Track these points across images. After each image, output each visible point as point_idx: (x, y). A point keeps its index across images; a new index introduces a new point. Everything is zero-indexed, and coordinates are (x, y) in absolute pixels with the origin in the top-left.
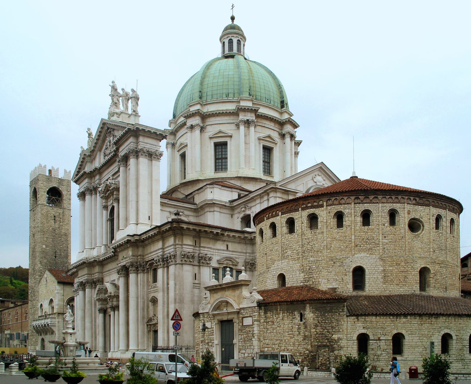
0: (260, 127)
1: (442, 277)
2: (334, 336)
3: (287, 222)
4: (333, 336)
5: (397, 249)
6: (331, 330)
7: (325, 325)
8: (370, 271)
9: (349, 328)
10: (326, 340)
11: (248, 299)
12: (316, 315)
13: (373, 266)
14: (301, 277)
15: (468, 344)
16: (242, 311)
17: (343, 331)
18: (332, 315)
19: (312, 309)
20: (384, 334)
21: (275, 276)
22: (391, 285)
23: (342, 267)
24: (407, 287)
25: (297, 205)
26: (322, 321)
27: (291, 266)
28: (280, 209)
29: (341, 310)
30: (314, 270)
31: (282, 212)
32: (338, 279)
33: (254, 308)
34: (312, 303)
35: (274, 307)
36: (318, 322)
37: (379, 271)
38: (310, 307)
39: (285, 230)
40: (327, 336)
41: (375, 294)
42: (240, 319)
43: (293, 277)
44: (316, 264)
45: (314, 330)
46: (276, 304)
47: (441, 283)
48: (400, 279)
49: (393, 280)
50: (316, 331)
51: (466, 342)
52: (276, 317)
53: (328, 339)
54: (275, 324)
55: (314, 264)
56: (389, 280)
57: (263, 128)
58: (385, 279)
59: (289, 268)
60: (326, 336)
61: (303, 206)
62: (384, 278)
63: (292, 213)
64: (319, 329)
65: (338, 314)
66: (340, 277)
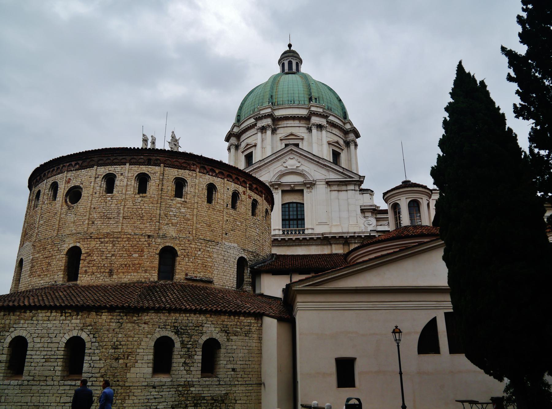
1: (102, 256)
24: (48, 279)
47: (99, 265)
48: (42, 268)
57: (285, 128)
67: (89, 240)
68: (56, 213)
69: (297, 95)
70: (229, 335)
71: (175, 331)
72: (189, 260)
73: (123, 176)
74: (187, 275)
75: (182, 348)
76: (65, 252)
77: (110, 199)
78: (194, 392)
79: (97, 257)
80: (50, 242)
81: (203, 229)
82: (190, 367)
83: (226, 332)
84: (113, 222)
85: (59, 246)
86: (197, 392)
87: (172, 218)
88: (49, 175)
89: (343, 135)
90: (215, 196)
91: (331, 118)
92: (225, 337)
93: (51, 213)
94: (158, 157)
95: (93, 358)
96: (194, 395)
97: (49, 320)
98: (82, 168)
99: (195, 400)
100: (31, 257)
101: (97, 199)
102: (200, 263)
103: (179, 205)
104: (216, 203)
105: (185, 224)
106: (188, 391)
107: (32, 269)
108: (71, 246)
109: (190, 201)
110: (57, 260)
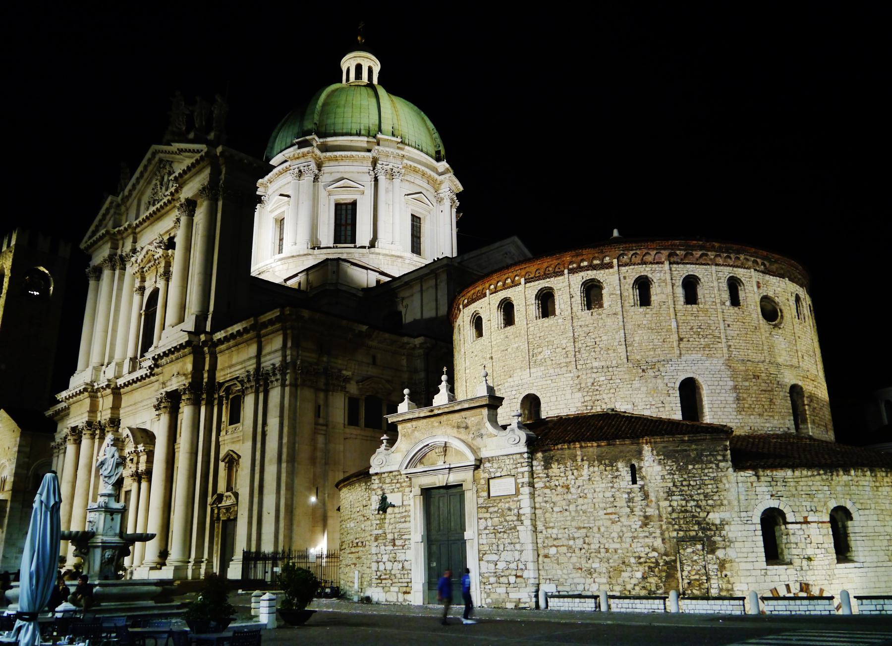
2: (711, 516)
3: (537, 297)
4: (709, 517)
6: (704, 503)
7: (688, 492)
8: (711, 387)
9: (742, 497)
10: (695, 524)
11: (504, 438)
12: (668, 468)
13: (715, 379)
14: (577, 400)
16: (487, 465)
17: (729, 503)
18: (702, 469)
19: (658, 455)
20: (813, 508)
21: (516, 400)
22: (750, 415)
23: (660, 378)
25: (559, 264)
26: (682, 481)
27: (551, 378)
28: (523, 273)
29: (720, 458)
30: (603, 385)
31: (527, 277)
32: (653, 403)
33: (518, 456)
34: (655, 442)
35: (567, 452)
36: (674, 485)
37: (726, 387)
38: (652, 450)
39: (533, 309)
40: (697, 517)
42: (483, 482)
43: (559, 399)
44: (607, 374)
45: (667, 503)
46: (572, 446)
48: (763, 405)
49: (753, 406)
50: (670, 506)
52: (573, 474)
53: (699, 523)
54: (572, 490)
55: (603, 374)
56: (746, 405)
59: (550, 382)
60: (694, 516)
61: (571, 267)
63: (548, 280)
64: (677, 501)
65: (714, 466)
66: (657, 399)
80: (763, 369)
88: (720, 261)
93: (747, 324)
98: (767, 272)
100: (731, 383)
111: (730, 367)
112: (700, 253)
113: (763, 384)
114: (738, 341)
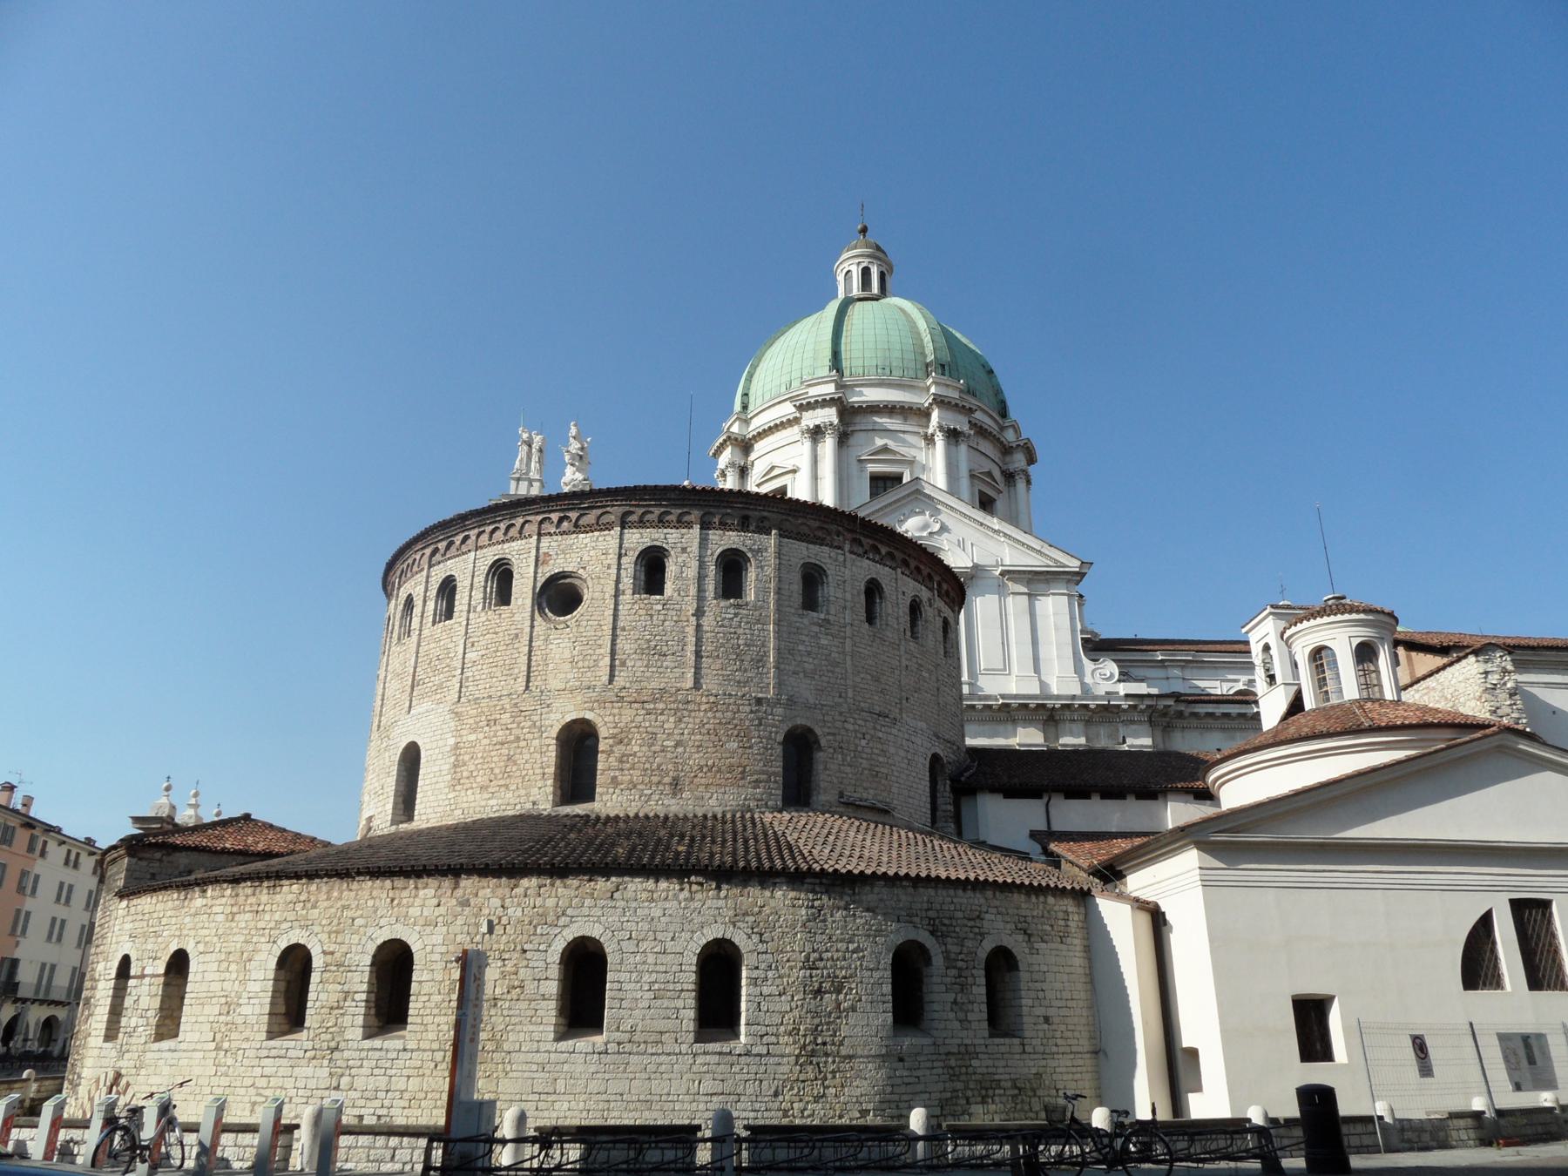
0: (861, 434)
1: (652, 745)
5: (499, 674)
15: (365, 987)
24: (510, 795)
41: (429, 825)
47: (647, 766)
51: (357, 977)
56: (465, 774)
58: (455, 772)
62: (452, 771)
67: (616, 705)
68: (517, 635)
69: (898, 354)
70: (1032, 940)
71: (931, 929)
72: (843, 760)
73: (686, 555)
74: (841, 795)
75: (947, 968)
76: (554, 732)
77: (659, 607)
78: (979, 1071)
79: (641, 746)
80: (507, 706)
81: (866, 686)
82: (967, 1012)
83: (1025, 933)
84: (673, 665)
85: (535, 718)
86: (985, 1071)
87: (804, 659)
89: (999, 455)
90: (881, 610)
91: (978, 415)
92: (1024, 944)
93: (501, 634)
94: (765, 514)
95: (766, 990)
96: (978, 1077)
97: (652, 900)
98: (578, 528)
99: (981, 1088)
100: (452, 741)
101: (630, 606)
102: (867, 766)
103: (816, 629)
104: (884, 627)
105: (830, 674)
106: (967, 1067)
107: (458, 770)
108: (568, 718)
109: (836, 619)
110: (532, 750)
111: (456, 713)
112: (460, 537)
113: (500, 733)
114: (480, 667)
